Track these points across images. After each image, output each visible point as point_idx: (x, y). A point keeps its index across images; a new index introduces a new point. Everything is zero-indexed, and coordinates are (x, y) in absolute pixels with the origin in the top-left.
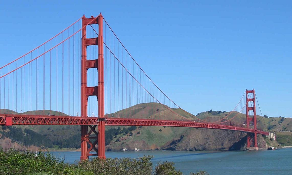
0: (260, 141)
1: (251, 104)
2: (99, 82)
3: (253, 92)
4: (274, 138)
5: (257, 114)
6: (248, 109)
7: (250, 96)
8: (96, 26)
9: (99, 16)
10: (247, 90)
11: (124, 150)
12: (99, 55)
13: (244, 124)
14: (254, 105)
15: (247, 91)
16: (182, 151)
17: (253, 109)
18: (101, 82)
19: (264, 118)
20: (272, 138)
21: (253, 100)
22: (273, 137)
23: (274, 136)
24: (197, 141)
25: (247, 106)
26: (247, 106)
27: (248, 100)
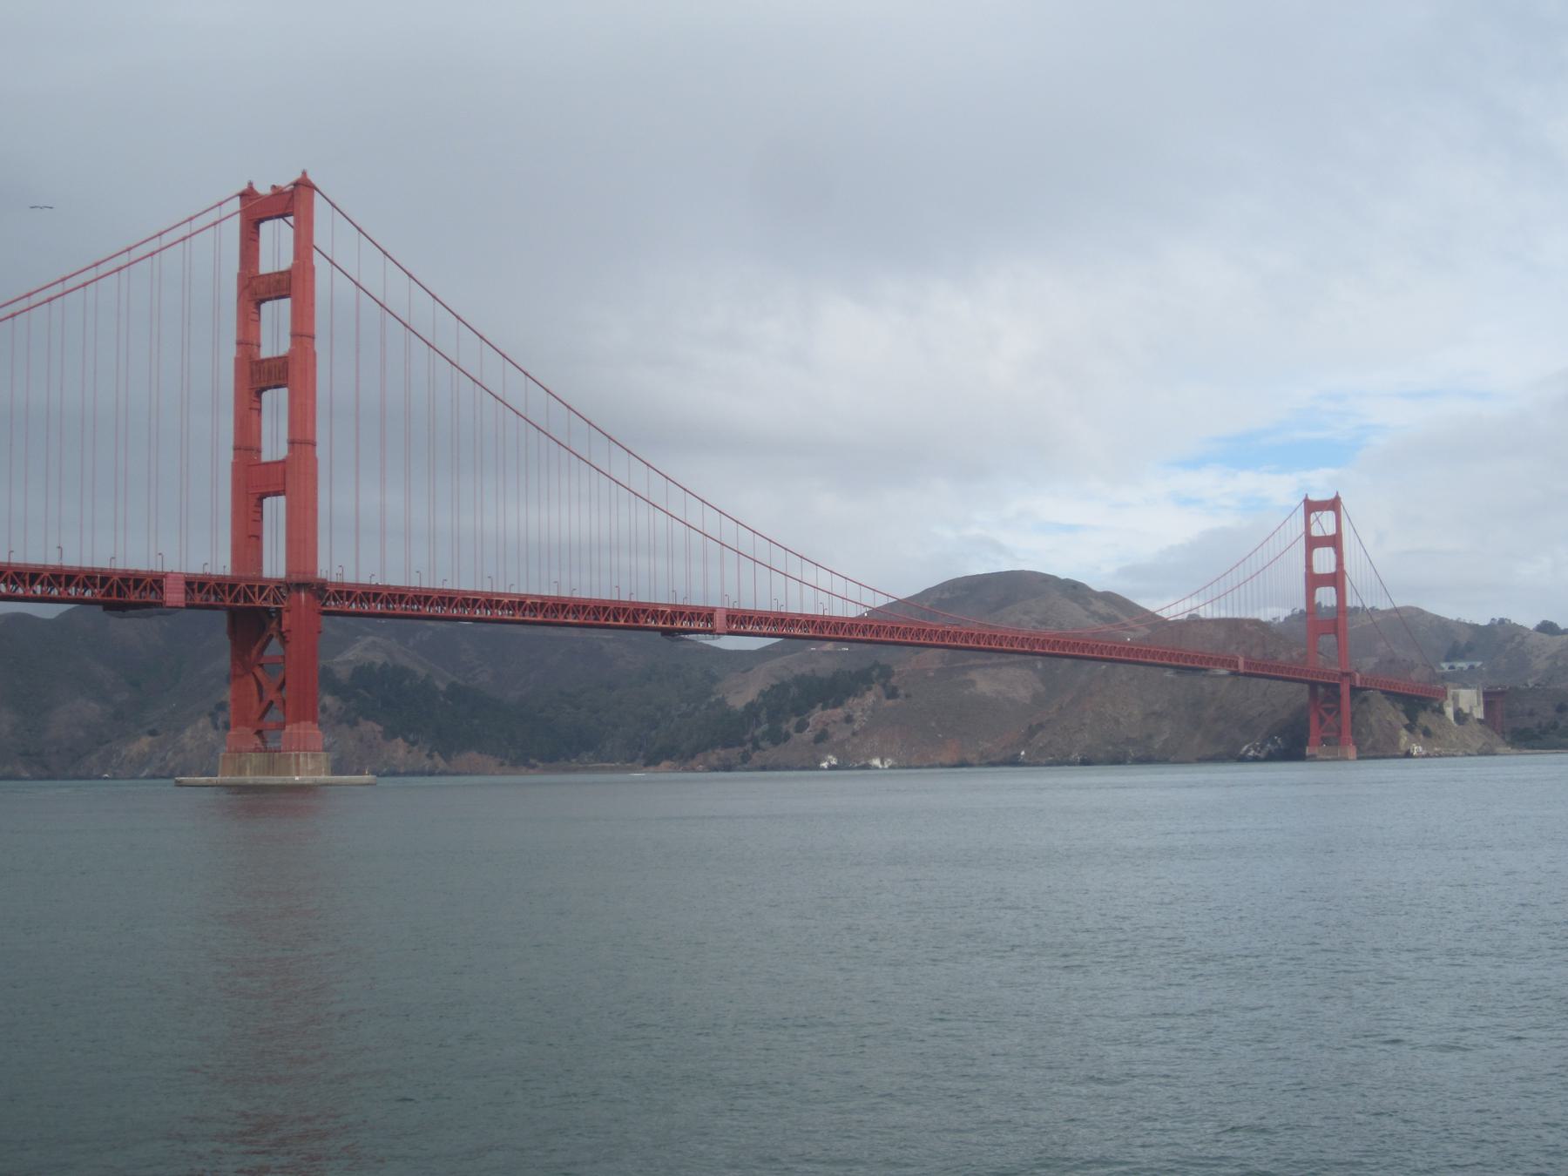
0: (1373, 720)
1: (1324, 561)
2: (292, 443)
3: (1334, 505)
4: (1479, 713)
5: (1351, 601)
6: (1314, 581)
7: (1324, 524)
8: (291, 219)
9: (296, 184)
10: (1311, 498)
11: (825, 765)
12: (295, 335)
13: (1447, 660)
14: (1340, 562)
15: (1307, 501)
16: (1050, 764)
17: (1336, 579)
18: (302, 442)
19: (1539, 634)
20: (1466, 710)
21: (1335, 541)
22: (1471, 708)
23: (1479, 704)
24: (1117, 722)
25: (1309, 565)
26: (1309, 565)
27: (1312, 543)
